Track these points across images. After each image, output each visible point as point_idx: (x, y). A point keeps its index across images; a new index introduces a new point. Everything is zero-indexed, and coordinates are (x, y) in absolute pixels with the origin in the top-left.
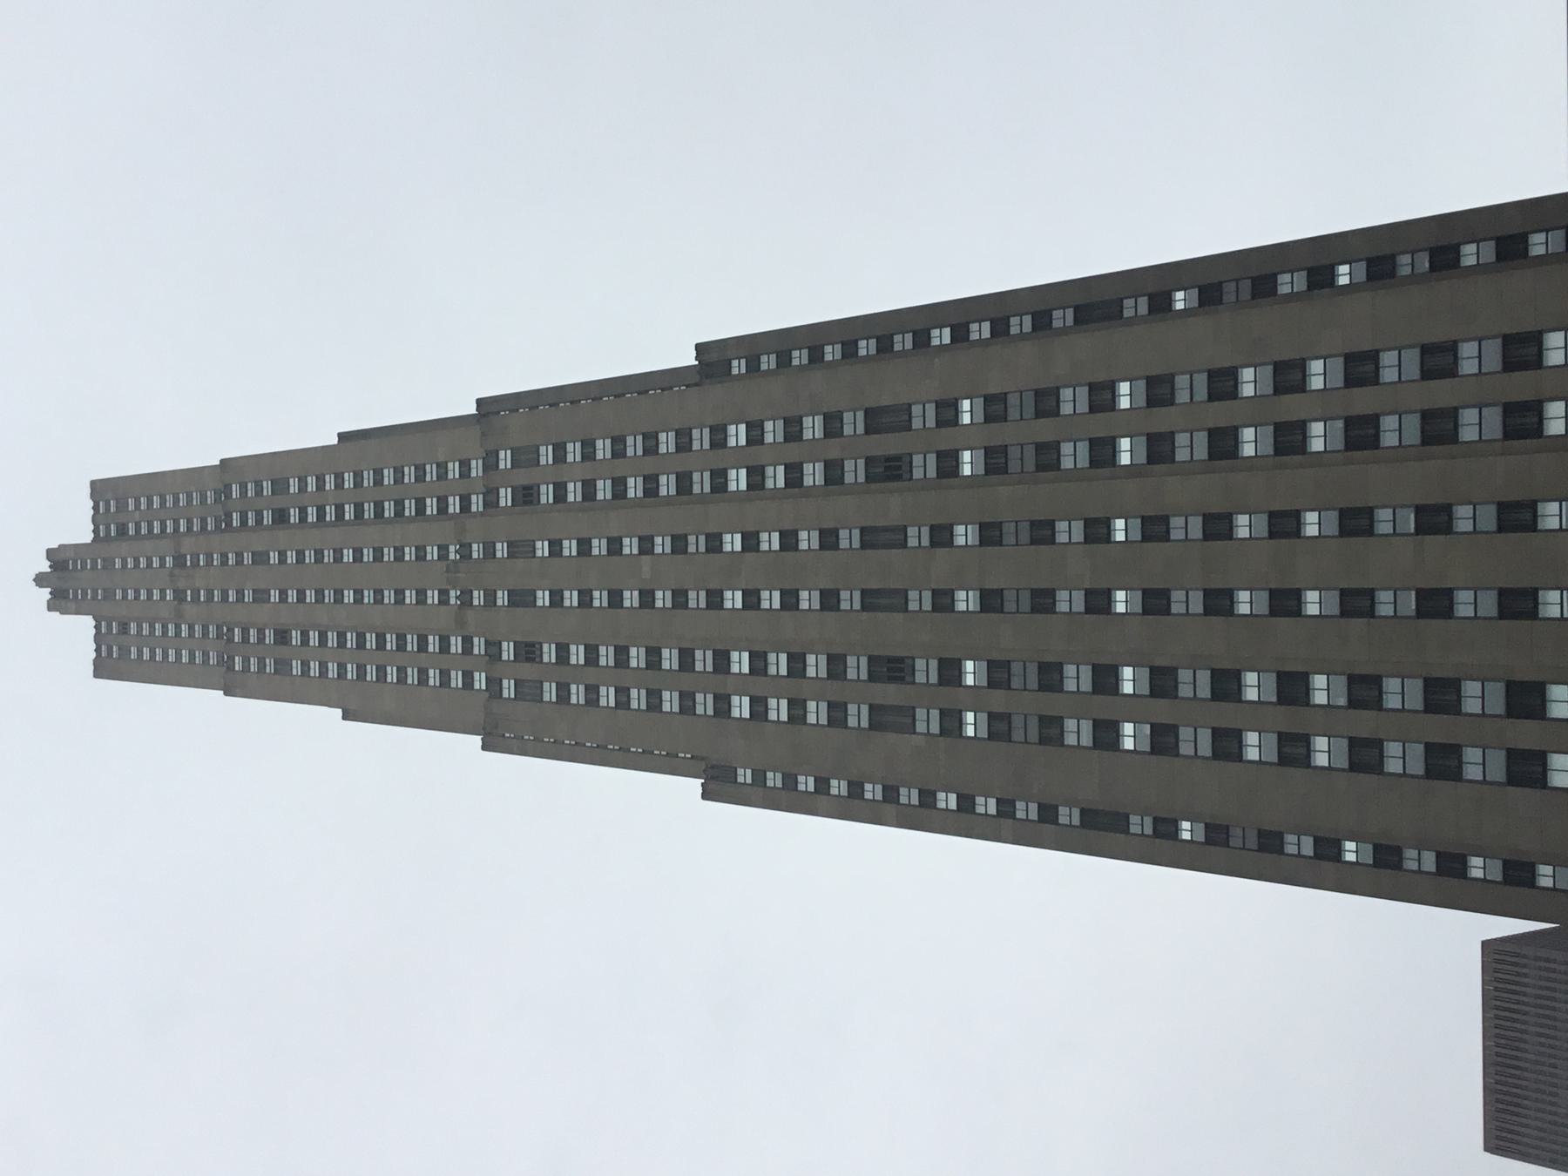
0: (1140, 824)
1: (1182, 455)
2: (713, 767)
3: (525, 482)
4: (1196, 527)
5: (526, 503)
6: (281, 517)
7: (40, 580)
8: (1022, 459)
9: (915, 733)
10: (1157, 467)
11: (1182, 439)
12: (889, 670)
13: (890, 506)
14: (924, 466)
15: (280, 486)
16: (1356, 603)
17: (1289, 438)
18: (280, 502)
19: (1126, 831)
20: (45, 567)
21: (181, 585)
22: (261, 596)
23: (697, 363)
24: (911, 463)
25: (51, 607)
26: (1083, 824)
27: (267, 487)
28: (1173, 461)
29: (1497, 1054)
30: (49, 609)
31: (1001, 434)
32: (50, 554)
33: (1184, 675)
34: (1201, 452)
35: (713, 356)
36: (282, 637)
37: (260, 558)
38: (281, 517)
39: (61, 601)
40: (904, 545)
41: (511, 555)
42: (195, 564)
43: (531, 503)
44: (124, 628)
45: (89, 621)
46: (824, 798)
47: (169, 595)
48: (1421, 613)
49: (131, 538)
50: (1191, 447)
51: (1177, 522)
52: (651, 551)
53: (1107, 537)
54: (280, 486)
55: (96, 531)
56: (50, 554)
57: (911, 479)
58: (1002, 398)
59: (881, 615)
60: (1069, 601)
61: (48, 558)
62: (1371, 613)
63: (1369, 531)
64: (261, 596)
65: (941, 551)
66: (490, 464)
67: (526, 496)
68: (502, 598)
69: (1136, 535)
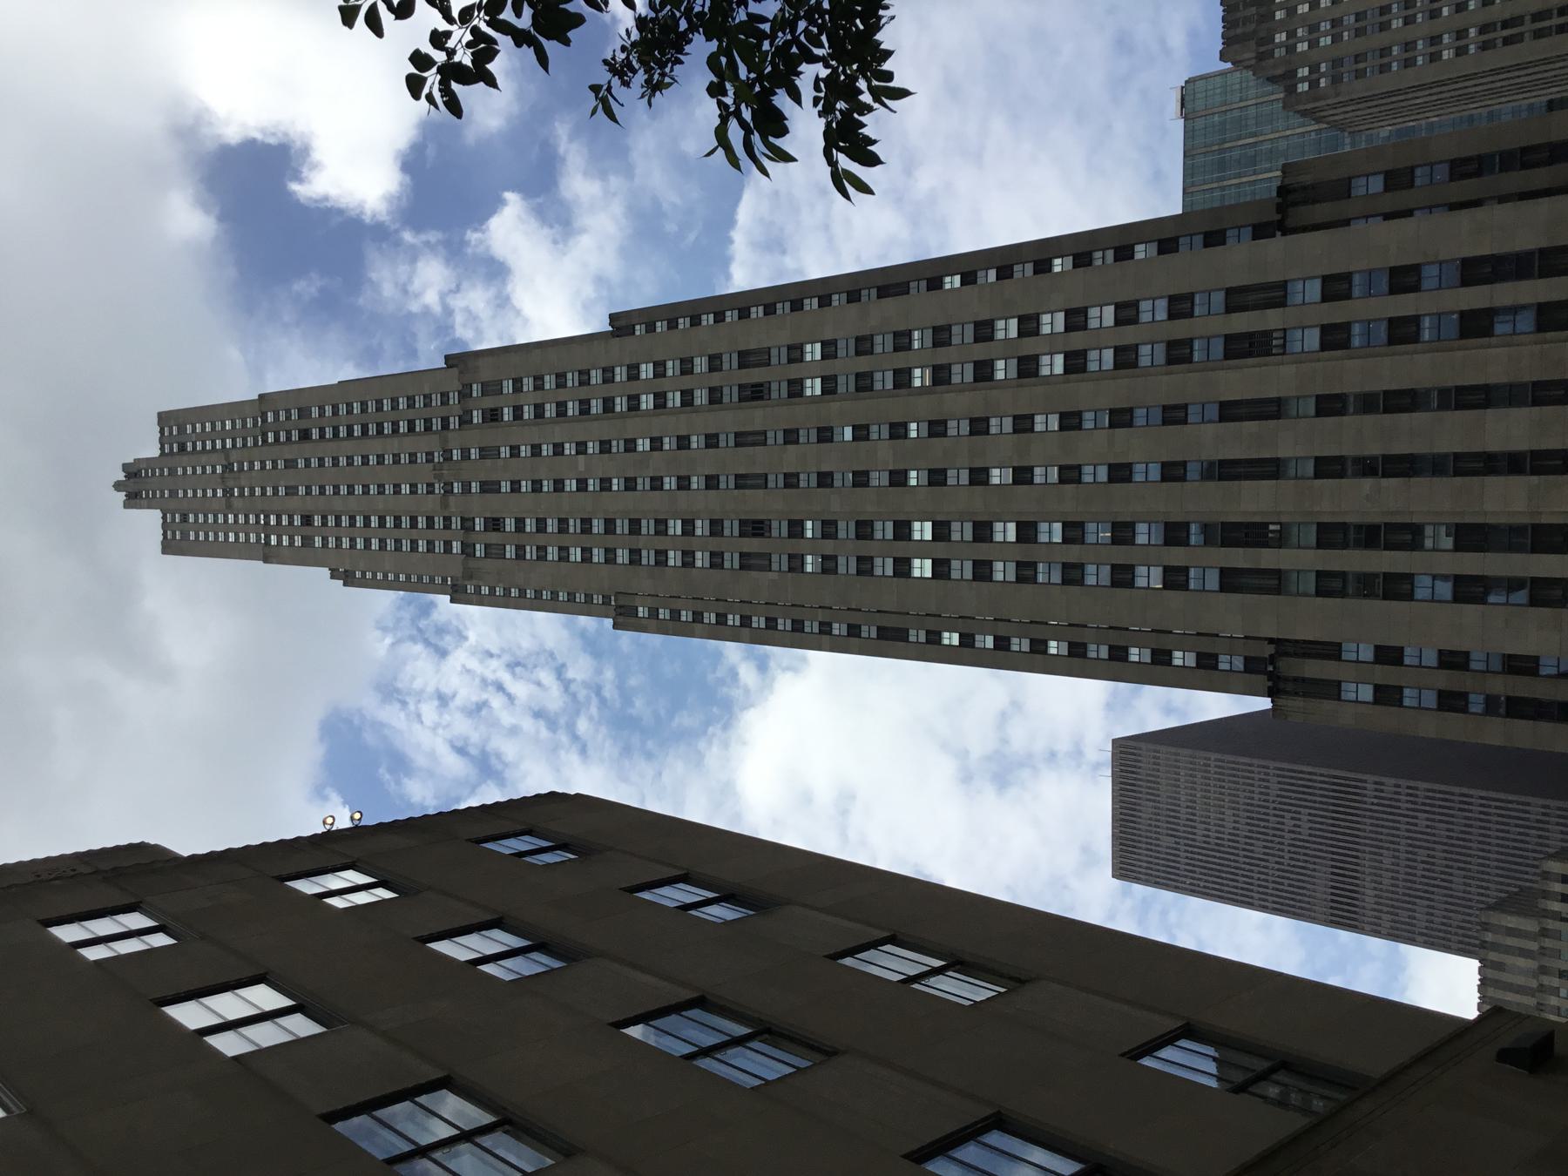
0: (917, 636)
1: (956, 379)
2: (621, 607)
4: (965, 427)
5: (492, 420)
6: (305, 435)
7: (118, 486)
8: (845, 384)
9: (770, 570)
10: (939, 388)
11: (956, 369)
12: (753, 528)
13: (755, 417)
14: (779, 390)
15: (304, 413)
16: (1070, 474)
17: (1028, 367)
18: (304, 424)
19: (907, 640)
20: (121, 476)
21: (230, 483)
22: (291, 491)
23: (611, 329)
24: (770, 388)
25: (127, 505)
26: (879, 637)
27: (294, 414)
28: (950, 384)
29: (1121, 814)
30: (125, 507)
31: (832, 367)
32: (125, 467)
33: (955, 526)
34: (969, 377)
35: (622, 323)
36: (307, 520)
37: (291, 464)
38: (305, 435)
39: (134, 499)
41: (482, 457)
42: (241, 469)
43: (496, 420)
44: (184, 518)
45: (157, 514)
46: (700, 625)
47: (220, 493)
48: (1111, 480)
50: (962, 373)
51: (952, 424)
52: (585, 452)
53: (906, 436)
54: (304, 413)
55: (162, 448)
56: (125, 467)
57: (770, 399)
58: (834, 343)
59: (747, 492)
60: (879, 479)
62: (1079, 481)
63: (1079, 427)
64: (291, 491)
65: (791, 447)
67: (493, 416)
68: (475, 487)
69: (925, 433)
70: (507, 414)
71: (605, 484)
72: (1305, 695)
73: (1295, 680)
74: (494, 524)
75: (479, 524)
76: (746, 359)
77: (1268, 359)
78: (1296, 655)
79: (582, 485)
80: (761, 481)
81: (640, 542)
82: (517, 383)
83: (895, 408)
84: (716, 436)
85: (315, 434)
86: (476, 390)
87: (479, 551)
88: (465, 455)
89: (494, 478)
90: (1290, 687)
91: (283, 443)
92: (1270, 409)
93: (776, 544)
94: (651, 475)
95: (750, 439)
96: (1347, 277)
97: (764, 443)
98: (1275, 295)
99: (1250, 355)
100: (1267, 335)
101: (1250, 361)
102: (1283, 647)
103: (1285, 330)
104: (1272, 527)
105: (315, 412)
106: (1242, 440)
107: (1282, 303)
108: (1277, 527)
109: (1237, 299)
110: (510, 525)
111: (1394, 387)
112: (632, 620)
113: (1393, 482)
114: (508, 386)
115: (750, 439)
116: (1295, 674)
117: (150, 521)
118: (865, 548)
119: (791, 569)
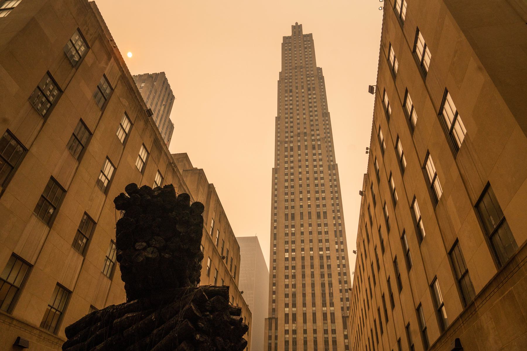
2: (277, 170)
3: (316, 147)
7: (297, 23)
13: (314, 216)
18: (311, 89)
20: (299, 24)
25: (292, 26)
27: (313, 86)
30: (292, 26)
32: (301, 25)
39: (293, 27)
40: (309, 219)
43: (313, 149)
49: (304, 43)
52: (307, 174)
56: (301, 25)
59: (300, 215)
61: (300, 25)
65: (308, 225)
66: (319, 140)
70: (314, 151)
71: (300, 179)
72: (269, 324)
73: (272, 322)
74: (292, 149)
75: (292, 145)
76: (325, 213)
77: (323, 321)
78: (276, 322)
79: (300, 173)
80: (302, 218)
81: (289, 188)
82: (320, 154)
83: (316, 249)
84: (310, 207)
85: (309, 92)
86: (319, 143)
87: (286, 145)
88: (306, 141)
89: (301, 149)
90: (270, 321)
91: (307, 83)
92: (314, 321)
93: (290, 222)
94: (303, 191)
95: (310, 215)
96: (335, 333)
97: (309, 219)
98: (333, 321)
99: (323, 317)
100: (327, 320)
101: (322, 317)
102: (276, 319)
103: (327, 323)
104: (296, 322)
105: (314, 92)
106: (309, 317)
107: (332, 322)
108: (296, 323)
109: (332, 314)
110: (292, 153)
111: (318, 342)
112: (274, 173)
113: (303, 342)
114: (320, 152)
115: (310, 215)
116: (273, 322)
117: (289, 33)
118: (290, 243)
119: (285, 226)
